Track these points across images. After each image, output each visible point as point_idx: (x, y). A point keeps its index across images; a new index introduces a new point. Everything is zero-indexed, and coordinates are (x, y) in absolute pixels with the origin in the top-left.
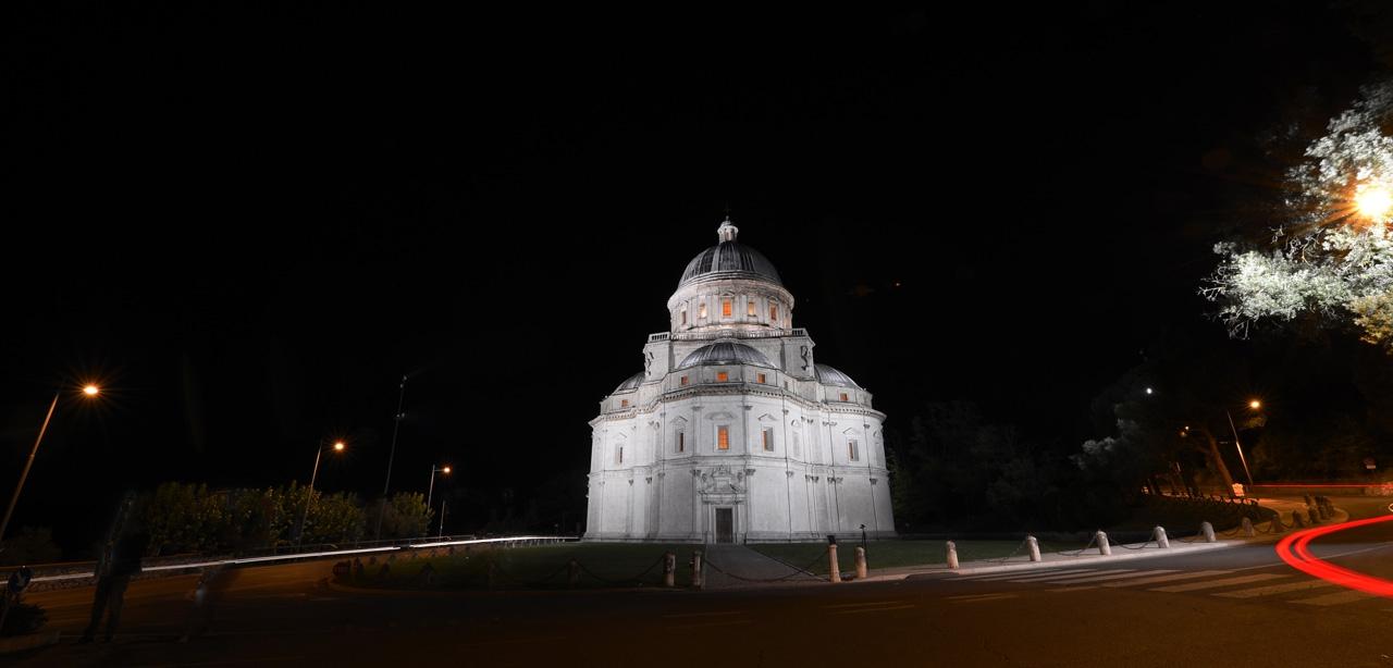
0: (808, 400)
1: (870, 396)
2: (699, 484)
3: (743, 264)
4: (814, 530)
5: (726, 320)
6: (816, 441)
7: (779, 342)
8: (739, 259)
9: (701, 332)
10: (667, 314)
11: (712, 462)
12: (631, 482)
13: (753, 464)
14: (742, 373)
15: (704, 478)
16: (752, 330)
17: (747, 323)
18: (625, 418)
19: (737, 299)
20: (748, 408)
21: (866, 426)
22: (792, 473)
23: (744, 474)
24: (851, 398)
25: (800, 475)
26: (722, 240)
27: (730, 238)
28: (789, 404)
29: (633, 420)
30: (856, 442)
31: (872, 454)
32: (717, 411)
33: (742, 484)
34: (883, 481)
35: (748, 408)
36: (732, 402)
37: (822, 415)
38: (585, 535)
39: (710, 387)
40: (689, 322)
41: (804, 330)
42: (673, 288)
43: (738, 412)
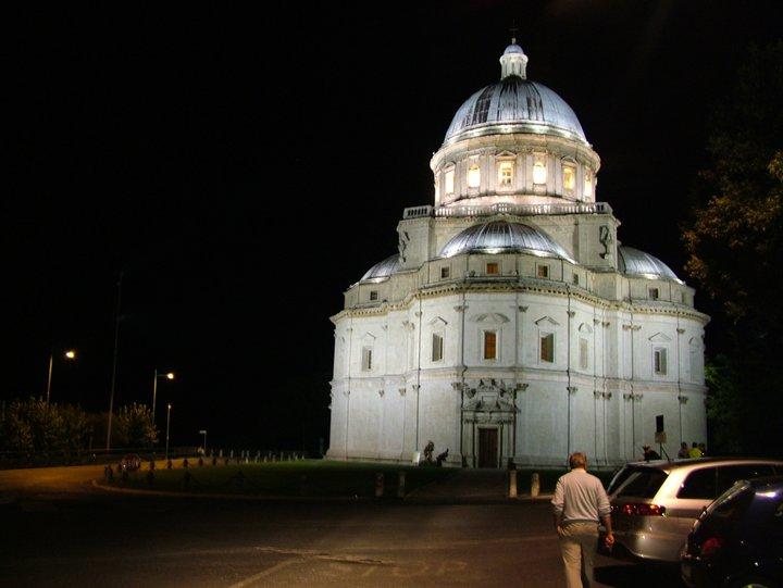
0: (606, 298)
1: (690, 293)
4: (600, 456)
5: (506, 189)
7: (570, 220)
9: (473, 205)
10: (429, 177)
12: (382, 393)
13: (527, 378)
14: (517, 264)
16: (538, 203)
17: (533, 193)
18: (375, 314)
19: (520, 161)
20: (522, 309)
21: (680, 331)
22: (574, 389)
24: (662, 294)
25: (585, 390)
26: (507, 72)
27: (517, 72)
28: (578, 305)
29: (384, 318)
30: (664, 351)
31: (685, 365)
32: (485, 312)
34: (697, 399)
35: (522, 309)
36: (503, 301)
37: (622, 316)
38: (328, 452)
39: (478, 282)
41: (606, 205)
42: (438, 143)
43: (510, 314)
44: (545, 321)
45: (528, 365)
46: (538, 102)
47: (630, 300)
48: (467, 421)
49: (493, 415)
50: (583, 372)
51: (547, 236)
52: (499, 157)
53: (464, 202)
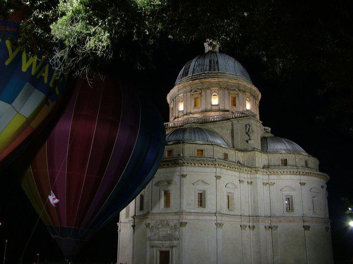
0: (251, 167)
1: (313, 162)
2: (149, 234)
3: (210, 66)
5: (196, 110)
6: (254, 198)
8: (208, 63)
11: (158, 217)
13: (186, 218)
15: (152, 229)
16: (214, 115)
17: (211, 111)
19: (203, 93)
20: (183, 176)
21: (302, 184)
23: (178, 225)
24: (289, 162)
25: (231, 226)
33: (177, 233)
37: (261, 177)
40: (174, 115)
44: (200, 183)
45: (188, 211)
46: (216, 61)
47: (267, 167)
48: (153, 247)
49: (167, 242)
50: (230, 213)
51: (217, 133)
52: (192, 93)
53: (177, 120)
